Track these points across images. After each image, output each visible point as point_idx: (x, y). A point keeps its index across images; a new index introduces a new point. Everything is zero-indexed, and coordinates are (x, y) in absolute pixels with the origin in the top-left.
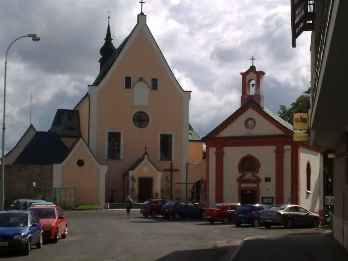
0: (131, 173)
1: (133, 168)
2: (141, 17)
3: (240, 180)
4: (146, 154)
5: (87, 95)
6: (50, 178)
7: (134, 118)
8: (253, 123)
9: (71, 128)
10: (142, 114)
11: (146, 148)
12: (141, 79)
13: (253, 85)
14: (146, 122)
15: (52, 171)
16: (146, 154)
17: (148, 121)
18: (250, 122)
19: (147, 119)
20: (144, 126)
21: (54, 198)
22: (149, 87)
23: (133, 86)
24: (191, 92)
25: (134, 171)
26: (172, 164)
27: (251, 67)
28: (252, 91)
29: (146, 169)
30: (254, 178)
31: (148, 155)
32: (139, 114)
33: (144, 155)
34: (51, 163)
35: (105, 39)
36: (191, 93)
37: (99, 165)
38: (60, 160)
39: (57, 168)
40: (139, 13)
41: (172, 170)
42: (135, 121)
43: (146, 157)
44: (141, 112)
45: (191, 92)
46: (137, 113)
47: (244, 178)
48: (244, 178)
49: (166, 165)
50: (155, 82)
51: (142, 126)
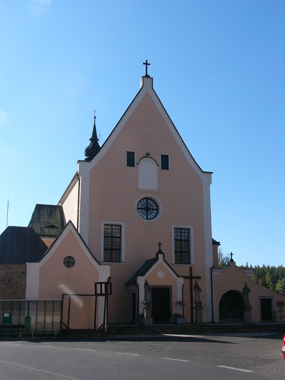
0: (141, 281)
1: (143, 271)
4: (160, 252)
5: (77, 175)
9: (52, 227)
10: (149, 201)
12: (148, 155)
14: (155, 212)
16: (160, 252)
17: (157, 210)
19: (155, 208)
20: (152, 217)
22: (158, 166)
23: (138, 164)
25: (145, 276)
26: (191, 268)
29: (161, 275)
31: (163, 254)
32: (145, 200)
33: (157, 255)
35: (90, 140)
37: (97, 264)
38: (37, 258)
41: (190, 277)
42: (139, 210)
43: (161, 256)
44: (147, 199)
45: (212, 173)
46: (143, 199)
49: (184, 269)
50: (165, 160)
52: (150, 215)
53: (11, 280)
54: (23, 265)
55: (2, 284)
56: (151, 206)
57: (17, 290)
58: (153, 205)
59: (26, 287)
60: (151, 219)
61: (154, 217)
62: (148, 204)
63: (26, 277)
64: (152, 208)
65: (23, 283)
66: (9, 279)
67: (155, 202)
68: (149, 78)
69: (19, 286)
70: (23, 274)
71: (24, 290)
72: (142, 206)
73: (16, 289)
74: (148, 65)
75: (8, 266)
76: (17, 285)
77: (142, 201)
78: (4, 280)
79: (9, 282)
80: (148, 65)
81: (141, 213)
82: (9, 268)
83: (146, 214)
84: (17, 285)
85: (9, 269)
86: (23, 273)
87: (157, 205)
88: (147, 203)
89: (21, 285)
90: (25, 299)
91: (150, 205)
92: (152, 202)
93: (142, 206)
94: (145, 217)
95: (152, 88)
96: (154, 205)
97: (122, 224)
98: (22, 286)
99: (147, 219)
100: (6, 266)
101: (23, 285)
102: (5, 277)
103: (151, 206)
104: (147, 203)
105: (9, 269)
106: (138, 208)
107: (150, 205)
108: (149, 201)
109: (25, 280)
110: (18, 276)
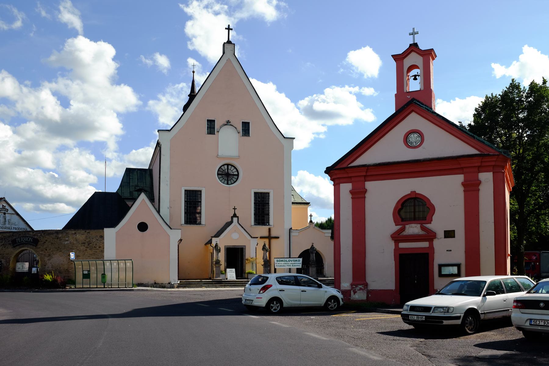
1: (218, 235)
2: (228, 46)
3: (397, 237)
6: (100, 247)
7: (220, 173)
8: (419, 139)
11: (235, 209)
13: (415, 76)
14: (236, 177)
15: (102, 237)
17: (238, 175)
18: (414, 138)
19: (236, 173)
20: (233, 182)
21: (102, 274)
24: (294, 138)
27: (411, 45)
28: (414, 86)
30: (422, 232)
34: (102, 227)
36: (294, 140)
39: (109, 233)
40: (226, 41)
42: (220, 176)
47: (404, 233)
48: (404, 233)
51: (229, 182)
52: (230, 180)
53: (91, 243)
54: (101, 230)
55: (83, 246)
56: (232, 172)
57: (96, 252)
58: (233, 171)
59: (104, 248)
60: (232, 184)
61: (235, 182)
62: (229, 170)
63: (104, 240)
64: (232, 174)
65: (101, 246)
66: (88, 242)
67: (235, 168)
68: (231, 45)
69: (98, 248)
70: (101, 238)
71: (103, 251)
72: (222, 172)
73: (95, 251)
74: (230, 30)
75: (88, 231)
76: (96, 247)
77: (222, 167)
78: (84, 243)
79: (89, 245)
80: (230, 30)
81: (221, 179)
82: (88, 233)
83: (226, 179)
84: (96, 247)
85: (89, 234)
86: (101, 237)
87: (237, 171)
88: (228, 169)
89: (100, 247)
90: (104, 259)
91: (231, 171)
92: (233, 168)
93: (222, 172)
94: (226, 182)
95: (234, 54)
96: (235, 170)
97: (202, 189)
98: (101, 248)
99: (228, 184)
100: (85, 231)
101: (101, 247)
102: (85, 240)
103: (232, 172)
104: (228, 169)
105: (89, 234)
106: (218, 174)
107: (231, 171)
108: (230, 167)
109: (103, 243)
110: (97, 240)
